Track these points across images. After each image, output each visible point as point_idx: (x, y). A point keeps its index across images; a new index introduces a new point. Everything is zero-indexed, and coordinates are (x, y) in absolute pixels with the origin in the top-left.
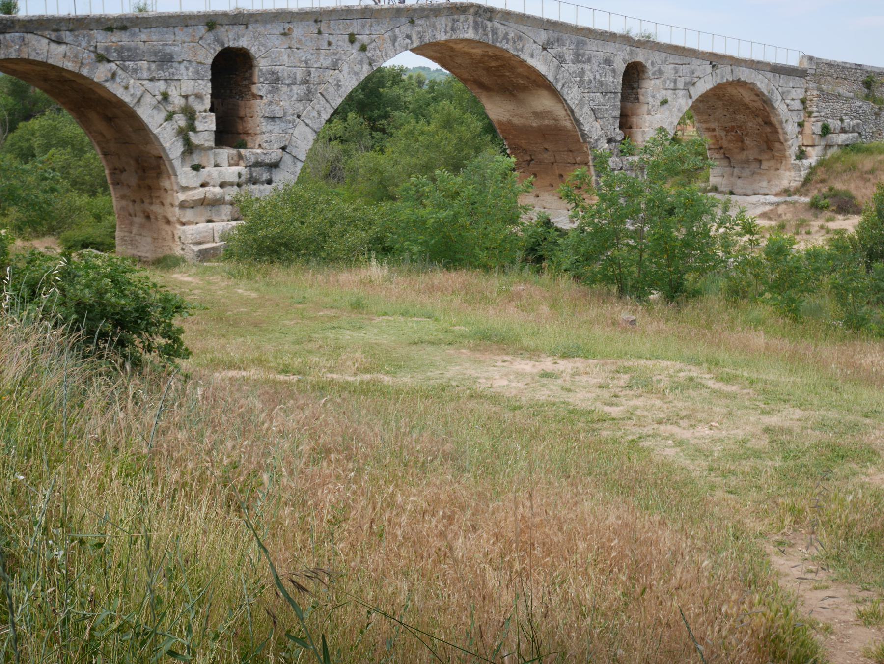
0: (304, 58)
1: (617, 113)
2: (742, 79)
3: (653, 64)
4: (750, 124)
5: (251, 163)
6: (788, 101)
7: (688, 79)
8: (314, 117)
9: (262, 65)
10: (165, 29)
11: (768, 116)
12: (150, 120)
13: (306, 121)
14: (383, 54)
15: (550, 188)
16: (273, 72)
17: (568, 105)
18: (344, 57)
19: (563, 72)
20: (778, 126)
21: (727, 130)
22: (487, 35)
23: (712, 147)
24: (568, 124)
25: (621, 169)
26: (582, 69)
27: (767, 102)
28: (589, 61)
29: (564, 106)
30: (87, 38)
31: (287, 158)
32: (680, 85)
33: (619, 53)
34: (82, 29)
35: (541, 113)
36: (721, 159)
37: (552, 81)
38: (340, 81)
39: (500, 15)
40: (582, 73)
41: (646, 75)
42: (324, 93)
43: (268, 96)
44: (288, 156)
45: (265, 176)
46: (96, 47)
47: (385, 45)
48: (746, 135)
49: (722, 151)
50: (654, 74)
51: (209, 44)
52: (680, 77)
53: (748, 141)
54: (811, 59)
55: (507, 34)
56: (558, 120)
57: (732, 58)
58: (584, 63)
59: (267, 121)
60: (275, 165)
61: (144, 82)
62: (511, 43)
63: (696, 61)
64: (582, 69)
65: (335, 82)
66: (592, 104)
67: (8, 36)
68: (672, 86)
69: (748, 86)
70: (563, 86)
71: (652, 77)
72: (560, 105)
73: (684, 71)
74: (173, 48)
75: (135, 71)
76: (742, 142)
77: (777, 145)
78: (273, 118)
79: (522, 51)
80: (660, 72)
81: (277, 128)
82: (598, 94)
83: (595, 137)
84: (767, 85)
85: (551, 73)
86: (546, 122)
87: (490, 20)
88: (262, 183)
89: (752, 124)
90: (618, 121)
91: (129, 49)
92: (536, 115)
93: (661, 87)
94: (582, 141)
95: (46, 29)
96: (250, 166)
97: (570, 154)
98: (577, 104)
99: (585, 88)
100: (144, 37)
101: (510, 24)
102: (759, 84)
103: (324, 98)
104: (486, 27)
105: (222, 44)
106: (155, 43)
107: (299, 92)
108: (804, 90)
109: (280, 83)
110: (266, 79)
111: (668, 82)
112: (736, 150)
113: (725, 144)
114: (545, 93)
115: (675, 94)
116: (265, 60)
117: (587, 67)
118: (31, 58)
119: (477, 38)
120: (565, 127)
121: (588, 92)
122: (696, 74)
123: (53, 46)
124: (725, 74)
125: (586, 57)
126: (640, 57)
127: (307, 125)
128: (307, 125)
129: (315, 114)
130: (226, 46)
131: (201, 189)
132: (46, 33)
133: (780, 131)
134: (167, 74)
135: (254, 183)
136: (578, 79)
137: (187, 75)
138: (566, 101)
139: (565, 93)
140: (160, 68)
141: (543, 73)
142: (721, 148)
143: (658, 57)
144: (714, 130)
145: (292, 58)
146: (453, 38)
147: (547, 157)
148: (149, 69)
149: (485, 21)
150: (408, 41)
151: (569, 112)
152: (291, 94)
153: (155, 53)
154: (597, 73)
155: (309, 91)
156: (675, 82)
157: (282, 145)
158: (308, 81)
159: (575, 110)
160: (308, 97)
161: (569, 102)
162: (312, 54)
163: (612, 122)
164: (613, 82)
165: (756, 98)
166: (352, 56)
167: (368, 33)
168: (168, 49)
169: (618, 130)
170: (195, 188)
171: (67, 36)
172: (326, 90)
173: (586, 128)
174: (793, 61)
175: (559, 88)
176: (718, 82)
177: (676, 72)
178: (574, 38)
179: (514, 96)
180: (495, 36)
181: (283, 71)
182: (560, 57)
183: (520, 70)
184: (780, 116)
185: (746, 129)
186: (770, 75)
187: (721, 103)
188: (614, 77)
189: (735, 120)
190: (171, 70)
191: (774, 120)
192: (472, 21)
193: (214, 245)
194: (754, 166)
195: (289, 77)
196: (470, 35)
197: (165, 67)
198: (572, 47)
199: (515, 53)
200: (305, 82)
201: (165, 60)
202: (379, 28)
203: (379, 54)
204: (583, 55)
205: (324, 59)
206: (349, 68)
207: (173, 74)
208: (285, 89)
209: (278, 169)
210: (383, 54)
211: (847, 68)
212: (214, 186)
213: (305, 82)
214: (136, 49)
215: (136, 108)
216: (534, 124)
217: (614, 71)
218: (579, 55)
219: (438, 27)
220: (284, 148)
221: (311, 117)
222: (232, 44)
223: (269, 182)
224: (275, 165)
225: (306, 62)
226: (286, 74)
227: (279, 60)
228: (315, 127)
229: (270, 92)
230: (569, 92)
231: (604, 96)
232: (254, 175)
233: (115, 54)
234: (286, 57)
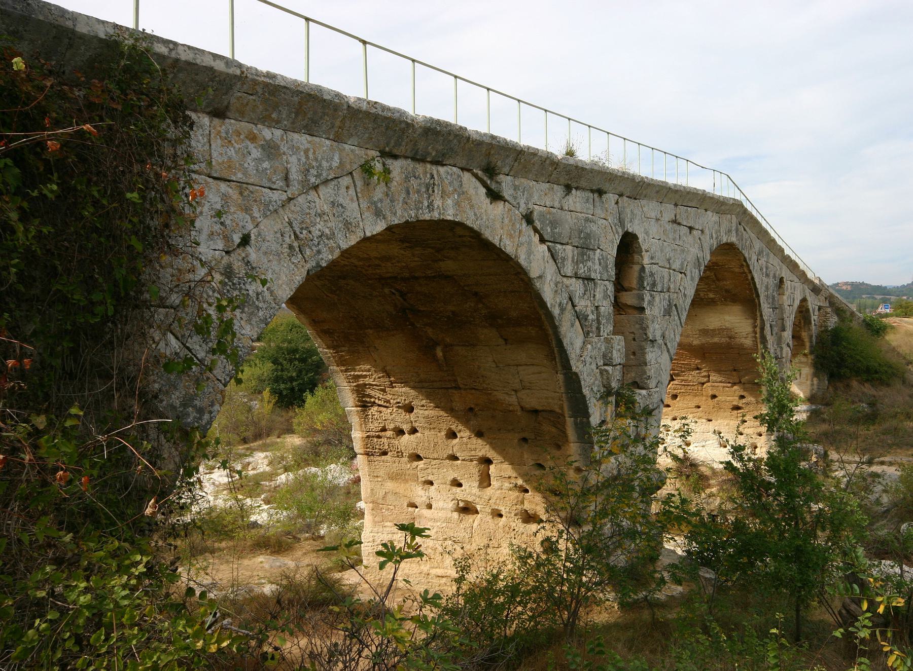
17: (763, 321)
35: (714, 330)
72: (750, 321)
86: (716, 340)
92: (705, 332)
97: (734, 373)
103: (677, 311)
114: (737, 309)
127: (668, 351)
129: (672, 336)
138: (761, 316)
151: (758, 330)
183: (728, 284)
216: (696, 342)
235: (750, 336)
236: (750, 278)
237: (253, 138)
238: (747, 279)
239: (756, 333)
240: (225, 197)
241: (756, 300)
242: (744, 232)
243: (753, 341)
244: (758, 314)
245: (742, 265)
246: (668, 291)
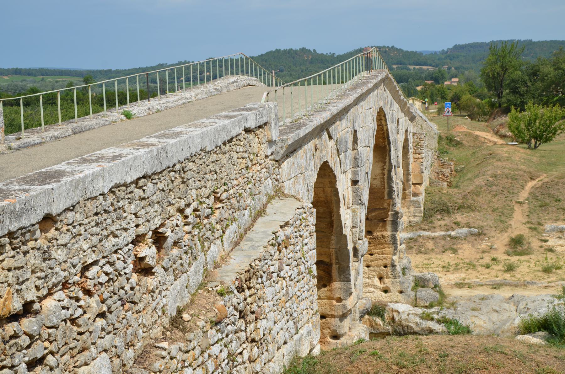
17: (390, 164)
29: (385, 165)
72: (381, 164)
94: (386, 197)
151: (386, 172)
184: (409, 159)
235: (378, 177)
236: (385, 129)
238: (383, 130)
239: (384, 175)
241: (387, 147)
242: (385, 92)
243: (381, 182)
244: (387, 160)
245: (381, 119)
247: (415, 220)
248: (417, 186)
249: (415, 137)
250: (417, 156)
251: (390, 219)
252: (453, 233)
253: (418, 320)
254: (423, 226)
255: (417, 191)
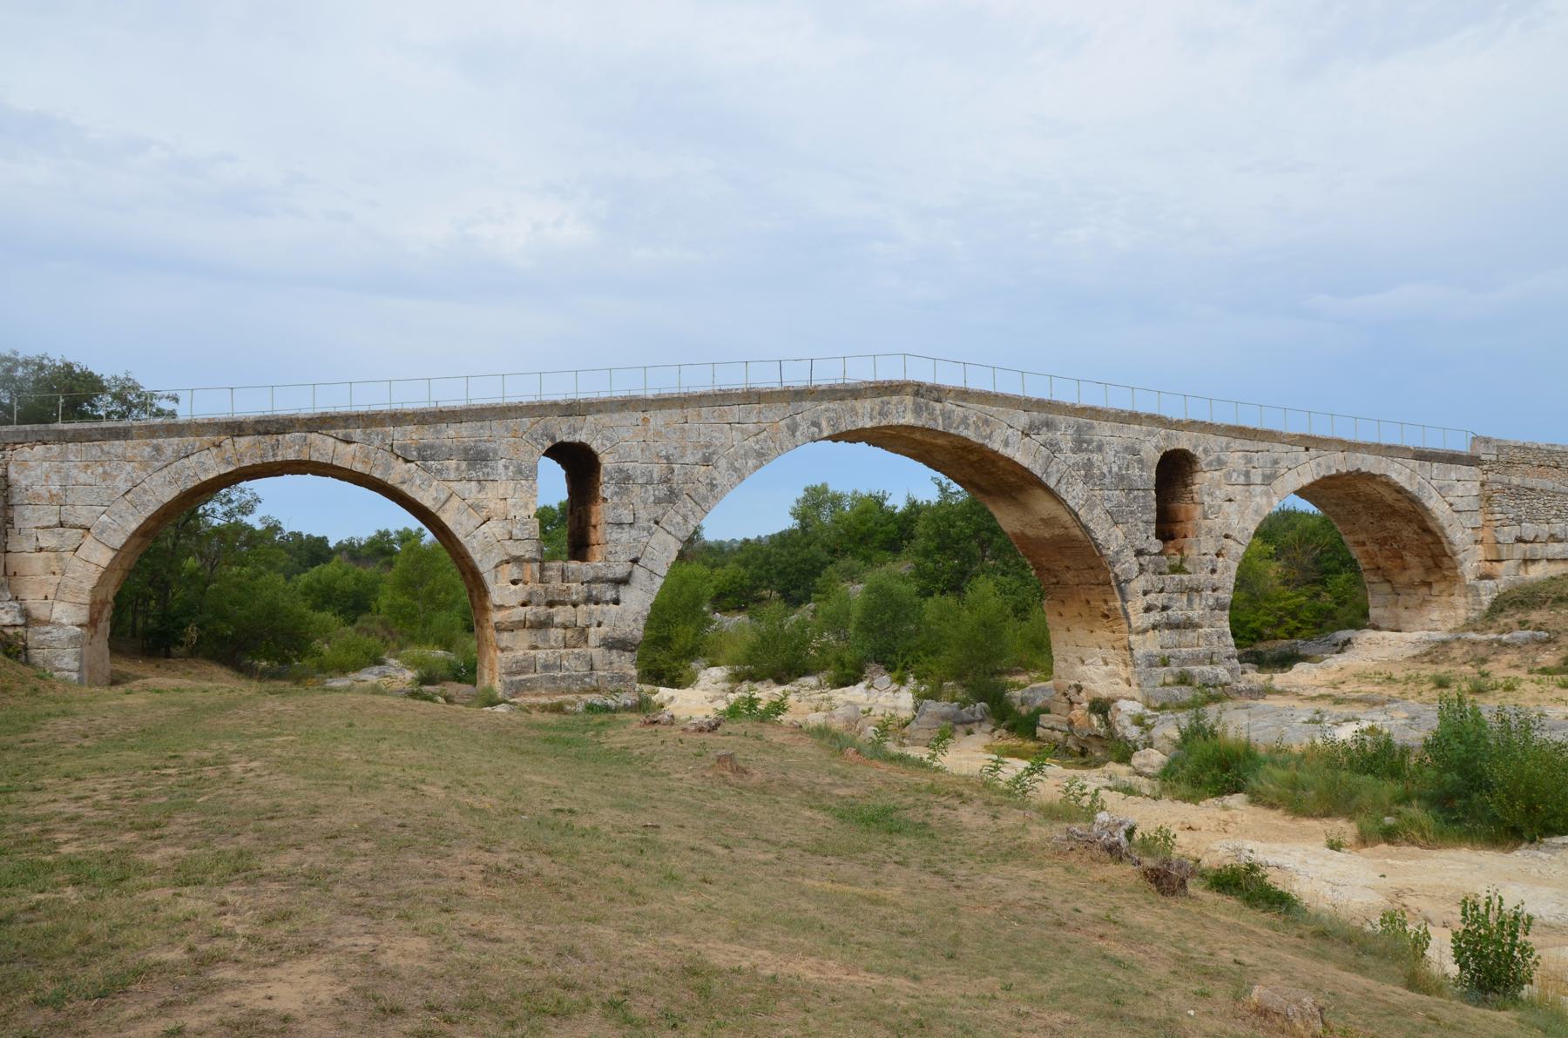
0: (664, 453)
1: (1153, 516)
2: (1363, 470)
3: (1205, 451)
4: (1405, 533)
5: (588, 579)
6: (1451, 500)
7: (1268, 471)
8: (678, 523)
9: (607, 462)
10: (479, 424)
11: (1423, 521)
12: (458, 527)
13: (666, 527)
14: (777, 446)
15: (1079, 619)
16: (621, 471)
18: (720, 451)
19: (1058, 464)
20: (1439, 534)
21: (1382, 543)
22: (935, 420)
23: (1367, 567)
24: (1077, 532)
25: (1161, 591)
26: (1089, 459)
27: (1413, 500)
28: (1100, 448)
30: (380, 436)
31: (639, 572)
32: (1257, 477)
33: (1149, 438)
34: (376, 426)
36: (1381, 582)
37: (1039, 475)
38: (715, 479)
39: (952, 394)
40: (1089, 465)
41: (1198, 467)
42: (693, 494)
43: (615, 498)
44: (641, 570)
45: (610, 594)
46: (392, 445)
47: (780, 435)
48: (1404, 548)
49: (1380, 572)
50: (1207, 465)
51: (536, 439)
52: (1254, 467)
53: (1410, 558)
54: (1487, 441)
55: (966, 417)
56: (1067, 528)
57: (1341, 442)
58: (1092, 452)
59: (612, 529)
60: (624, 581)
61: (451, 484)
62: (972, 428)
63: (1278, 447)
64: (1089, 459)
65: (708, 481)
66: (1107, 505)
67: (287, 436)
68: (1242, 479)
69: (1378, 479)
70: (1059, 481)
71: (1205, 469)
73: (1261, 461)
74: (488, 444)
75: (439, 471)
76: (1402, 558)
77: (1445, 560)
78: (620, 525)
79: (990, 438)
80: (1221, 463)
81: (625, 536)
82: (1118, 492)
83: (1114, 547)
84: (1411, 478)
85: (1038, 467)
86: (1057, 531)
87: (938, 400)
88: (607, 603)
89: (1408, 532)
90: (1154, 527)
91: (432, 447)
93: (1223, 481)
95: (333, 428)
96: (588, 582)
98: (1083, 506)
99: (1095, 484)
100: (451, 432)
101: (971, 405)
102: (1394, 476)
104: (934, 409)
105: (553, 438)
106: (466, 439)
107: (657, 493)
108: (1478, 484)
109: (631, 482)
110: (612, 479)
111: (1235, 475)
112: (1395, 571)
113: (1381, 562)
114: (1039, 492)
115: (1248, 491)
116: (611, 456)
117: (1096, 457)
118: (313, 459)
119: (920, 424)
120: (1077, 536)
121: (1101, 490)
122: (1283, 464)
123: (341, 446)
124: (1337, 463)
125: (1095, 444)
126: (1183, 441)
127: (669, 533)
128: (669, 533)
129: (679, 519)
130: (558, 441)
131: (521, 608)
132: (332, 432)
133: (1444, 540)
134: (480, 474)
135: (597, 603)
136: (1083, 472)
137: (506, 474)
138: (1065, 501)
139: (1062, 491)
140: (471, 467)
141: (1026, 466)
142: (1379, 568)
143: (1216, 442)
144: (1364, 544)
145: (647, 453)
146: (882, 424)
147: (1069, 577)
148: (457, 469)
149: (932, 402)
150: (816, 429)
152: (647, 496)
153: (466, 451)
154: (1113, 465)
155: (671, 491)
156: (1247, 474)
157: (632, 557)
158: (669, 480)
159: (1080, 513)
160: (672, 497)
161: (1069, 502)
162: (675, 448)
163: (1142, 529)
164: (1141, 476)
165: (1399, 497)
166: (732, 450)
167: (755, 421)
168: (483, 446)
169: (1153, 539)
170: (513, 607)
171: (357, 434)
172: (696, 489)
173: (1100, 536)
174: (1462, 446)
175: (1052, 483)
176: (1322, 474)
177: (1249, 461)
178: (1072, 420)
179: (1014, 498)
180: (946, 422)
181: (635, 468)
182: (1051, 445)
185: (1402, 540)
186: (1415, 464)
187: (1360, 505)
188: (1141, 469)
189: (1385, 529)
190: (486, 470)
191: (1431, 525)
192: (911, 404)
193: (535, 676)
194: (1423, 591)
195: (643, 474)
196: (909, 419)
197: (478, 466)
198: (1070, 431)
199: (980, 441)
200: (667, 481)
201: (477, 458)
202: (771, 415)
203: (772, 445)
204: (1089, 442)
205: (693, 453)
206: (727, 463)
207: (488, 474)
208: (636, 489)
209: (627, 586)
210: (777, 446)
211: (1558, 452)
212: (538, 605)
213: (667, 481)
214: (441, 447)
215: (439, 514)
216: (1047, 535)
217: (1141, 461)
218: (1085, 442)
219: (860, 411)
220: (635, 561)
221: (675, 521)
222: (566, 439)
223: (616, 602)
224: (624, 581)
225: (667, 458)
226: (639, 472)
227: (630, 455)
228: (680, 535)
229: (616, 493)
230: (1070, 489)
231: (1127, 494)
232: (594, 593)
233: (415, 453)
234: (639, 451)
237: (148, 445)
240: (133, 468)
246: (665, 482)
247: (1473, 615)
248: (1494, 563)
249: (1486, 488)
250: (1489, 517)
251: (1113, 583)
252: (1505, 637)
253: (1127, 722)
254: (1479, 626)
255: (1494, 572)
